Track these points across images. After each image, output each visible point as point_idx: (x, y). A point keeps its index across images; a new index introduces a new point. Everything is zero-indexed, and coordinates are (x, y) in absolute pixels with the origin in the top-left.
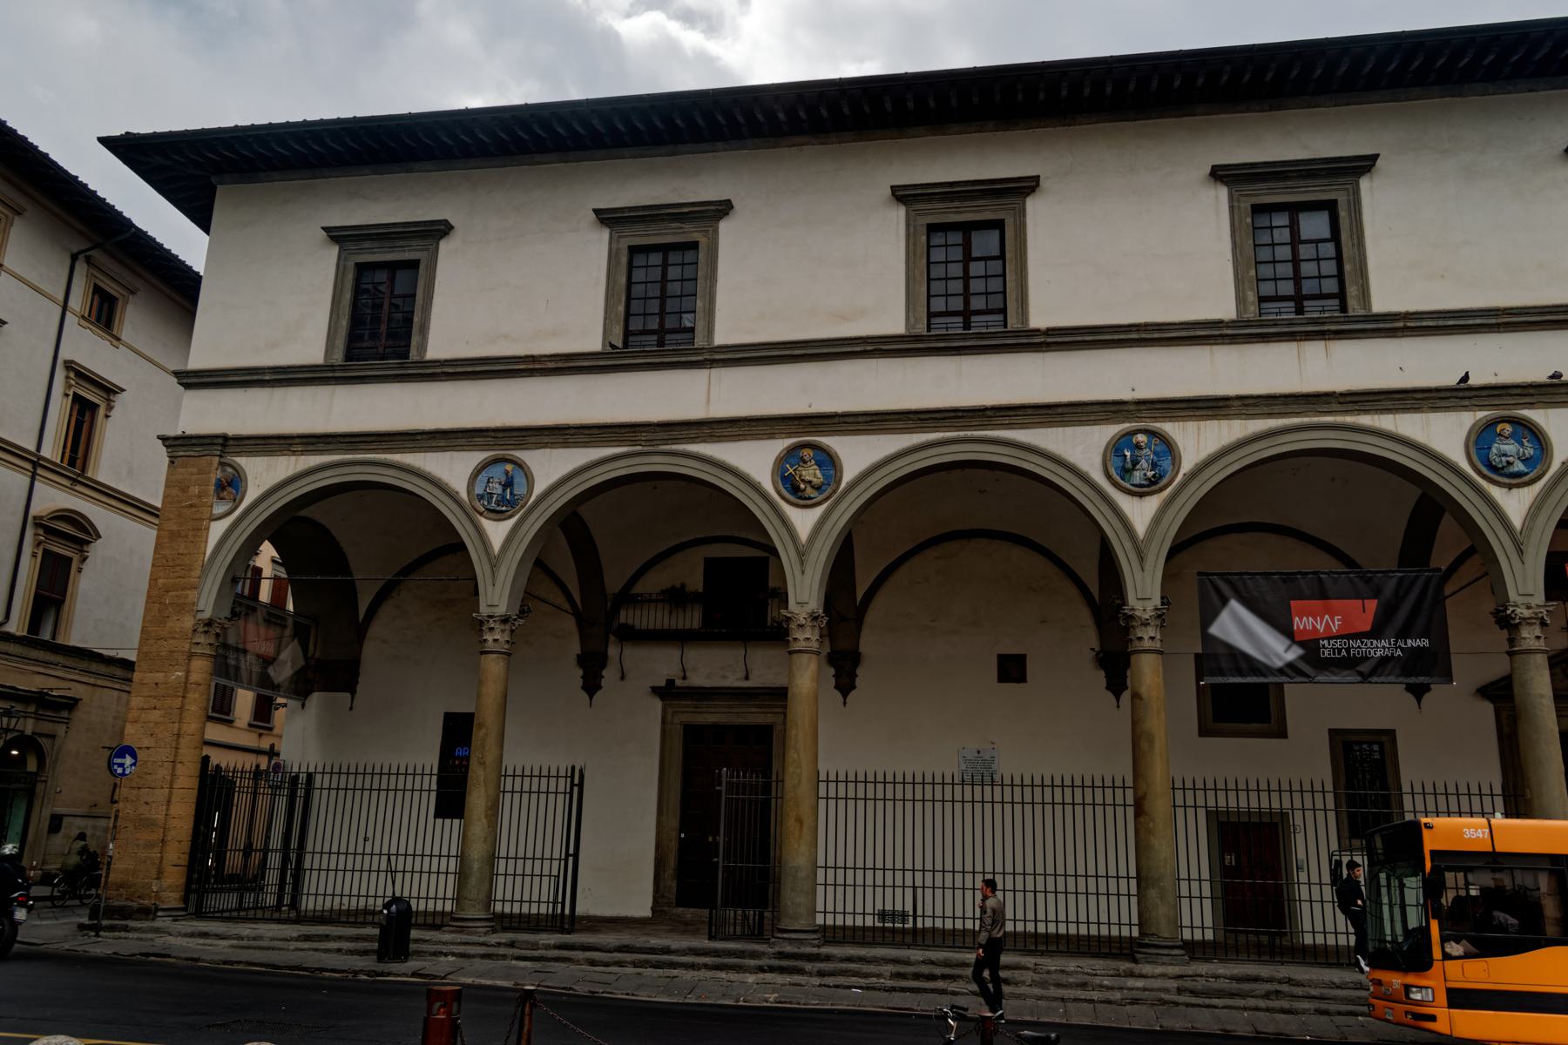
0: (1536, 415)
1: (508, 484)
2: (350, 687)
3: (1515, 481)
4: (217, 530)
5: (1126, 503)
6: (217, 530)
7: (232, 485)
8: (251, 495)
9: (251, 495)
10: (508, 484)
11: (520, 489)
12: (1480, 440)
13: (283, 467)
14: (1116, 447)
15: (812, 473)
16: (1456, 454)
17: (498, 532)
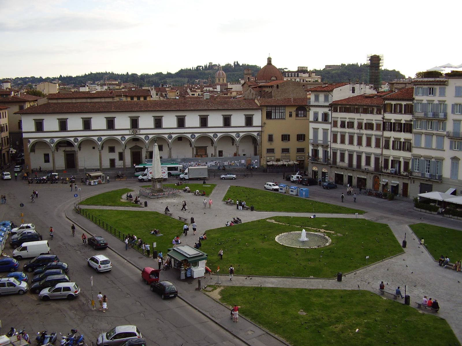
0: (125, 136)
1: (53, 141)
2: (34, 152)
3: (123, 141)
4: (29, 145)
5: (99, 142)
6: (29, 145)
7: (29, 142)
8: (31, 143)
9: (31, 143)
10: (53, 141)
11: (54, 141)
12: (122, 138)
13: (33, 140)
14: (98, 138)
15: (76, 140)
16: (120, 139)
17: (52, 145)
